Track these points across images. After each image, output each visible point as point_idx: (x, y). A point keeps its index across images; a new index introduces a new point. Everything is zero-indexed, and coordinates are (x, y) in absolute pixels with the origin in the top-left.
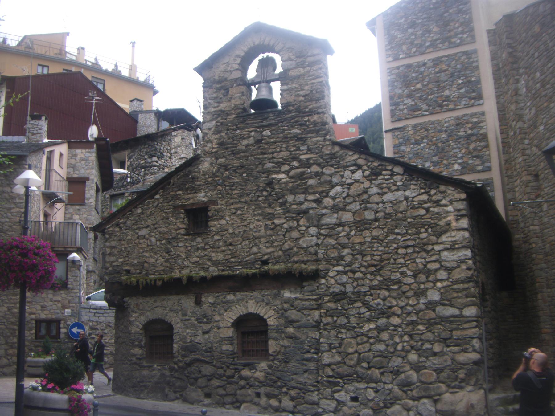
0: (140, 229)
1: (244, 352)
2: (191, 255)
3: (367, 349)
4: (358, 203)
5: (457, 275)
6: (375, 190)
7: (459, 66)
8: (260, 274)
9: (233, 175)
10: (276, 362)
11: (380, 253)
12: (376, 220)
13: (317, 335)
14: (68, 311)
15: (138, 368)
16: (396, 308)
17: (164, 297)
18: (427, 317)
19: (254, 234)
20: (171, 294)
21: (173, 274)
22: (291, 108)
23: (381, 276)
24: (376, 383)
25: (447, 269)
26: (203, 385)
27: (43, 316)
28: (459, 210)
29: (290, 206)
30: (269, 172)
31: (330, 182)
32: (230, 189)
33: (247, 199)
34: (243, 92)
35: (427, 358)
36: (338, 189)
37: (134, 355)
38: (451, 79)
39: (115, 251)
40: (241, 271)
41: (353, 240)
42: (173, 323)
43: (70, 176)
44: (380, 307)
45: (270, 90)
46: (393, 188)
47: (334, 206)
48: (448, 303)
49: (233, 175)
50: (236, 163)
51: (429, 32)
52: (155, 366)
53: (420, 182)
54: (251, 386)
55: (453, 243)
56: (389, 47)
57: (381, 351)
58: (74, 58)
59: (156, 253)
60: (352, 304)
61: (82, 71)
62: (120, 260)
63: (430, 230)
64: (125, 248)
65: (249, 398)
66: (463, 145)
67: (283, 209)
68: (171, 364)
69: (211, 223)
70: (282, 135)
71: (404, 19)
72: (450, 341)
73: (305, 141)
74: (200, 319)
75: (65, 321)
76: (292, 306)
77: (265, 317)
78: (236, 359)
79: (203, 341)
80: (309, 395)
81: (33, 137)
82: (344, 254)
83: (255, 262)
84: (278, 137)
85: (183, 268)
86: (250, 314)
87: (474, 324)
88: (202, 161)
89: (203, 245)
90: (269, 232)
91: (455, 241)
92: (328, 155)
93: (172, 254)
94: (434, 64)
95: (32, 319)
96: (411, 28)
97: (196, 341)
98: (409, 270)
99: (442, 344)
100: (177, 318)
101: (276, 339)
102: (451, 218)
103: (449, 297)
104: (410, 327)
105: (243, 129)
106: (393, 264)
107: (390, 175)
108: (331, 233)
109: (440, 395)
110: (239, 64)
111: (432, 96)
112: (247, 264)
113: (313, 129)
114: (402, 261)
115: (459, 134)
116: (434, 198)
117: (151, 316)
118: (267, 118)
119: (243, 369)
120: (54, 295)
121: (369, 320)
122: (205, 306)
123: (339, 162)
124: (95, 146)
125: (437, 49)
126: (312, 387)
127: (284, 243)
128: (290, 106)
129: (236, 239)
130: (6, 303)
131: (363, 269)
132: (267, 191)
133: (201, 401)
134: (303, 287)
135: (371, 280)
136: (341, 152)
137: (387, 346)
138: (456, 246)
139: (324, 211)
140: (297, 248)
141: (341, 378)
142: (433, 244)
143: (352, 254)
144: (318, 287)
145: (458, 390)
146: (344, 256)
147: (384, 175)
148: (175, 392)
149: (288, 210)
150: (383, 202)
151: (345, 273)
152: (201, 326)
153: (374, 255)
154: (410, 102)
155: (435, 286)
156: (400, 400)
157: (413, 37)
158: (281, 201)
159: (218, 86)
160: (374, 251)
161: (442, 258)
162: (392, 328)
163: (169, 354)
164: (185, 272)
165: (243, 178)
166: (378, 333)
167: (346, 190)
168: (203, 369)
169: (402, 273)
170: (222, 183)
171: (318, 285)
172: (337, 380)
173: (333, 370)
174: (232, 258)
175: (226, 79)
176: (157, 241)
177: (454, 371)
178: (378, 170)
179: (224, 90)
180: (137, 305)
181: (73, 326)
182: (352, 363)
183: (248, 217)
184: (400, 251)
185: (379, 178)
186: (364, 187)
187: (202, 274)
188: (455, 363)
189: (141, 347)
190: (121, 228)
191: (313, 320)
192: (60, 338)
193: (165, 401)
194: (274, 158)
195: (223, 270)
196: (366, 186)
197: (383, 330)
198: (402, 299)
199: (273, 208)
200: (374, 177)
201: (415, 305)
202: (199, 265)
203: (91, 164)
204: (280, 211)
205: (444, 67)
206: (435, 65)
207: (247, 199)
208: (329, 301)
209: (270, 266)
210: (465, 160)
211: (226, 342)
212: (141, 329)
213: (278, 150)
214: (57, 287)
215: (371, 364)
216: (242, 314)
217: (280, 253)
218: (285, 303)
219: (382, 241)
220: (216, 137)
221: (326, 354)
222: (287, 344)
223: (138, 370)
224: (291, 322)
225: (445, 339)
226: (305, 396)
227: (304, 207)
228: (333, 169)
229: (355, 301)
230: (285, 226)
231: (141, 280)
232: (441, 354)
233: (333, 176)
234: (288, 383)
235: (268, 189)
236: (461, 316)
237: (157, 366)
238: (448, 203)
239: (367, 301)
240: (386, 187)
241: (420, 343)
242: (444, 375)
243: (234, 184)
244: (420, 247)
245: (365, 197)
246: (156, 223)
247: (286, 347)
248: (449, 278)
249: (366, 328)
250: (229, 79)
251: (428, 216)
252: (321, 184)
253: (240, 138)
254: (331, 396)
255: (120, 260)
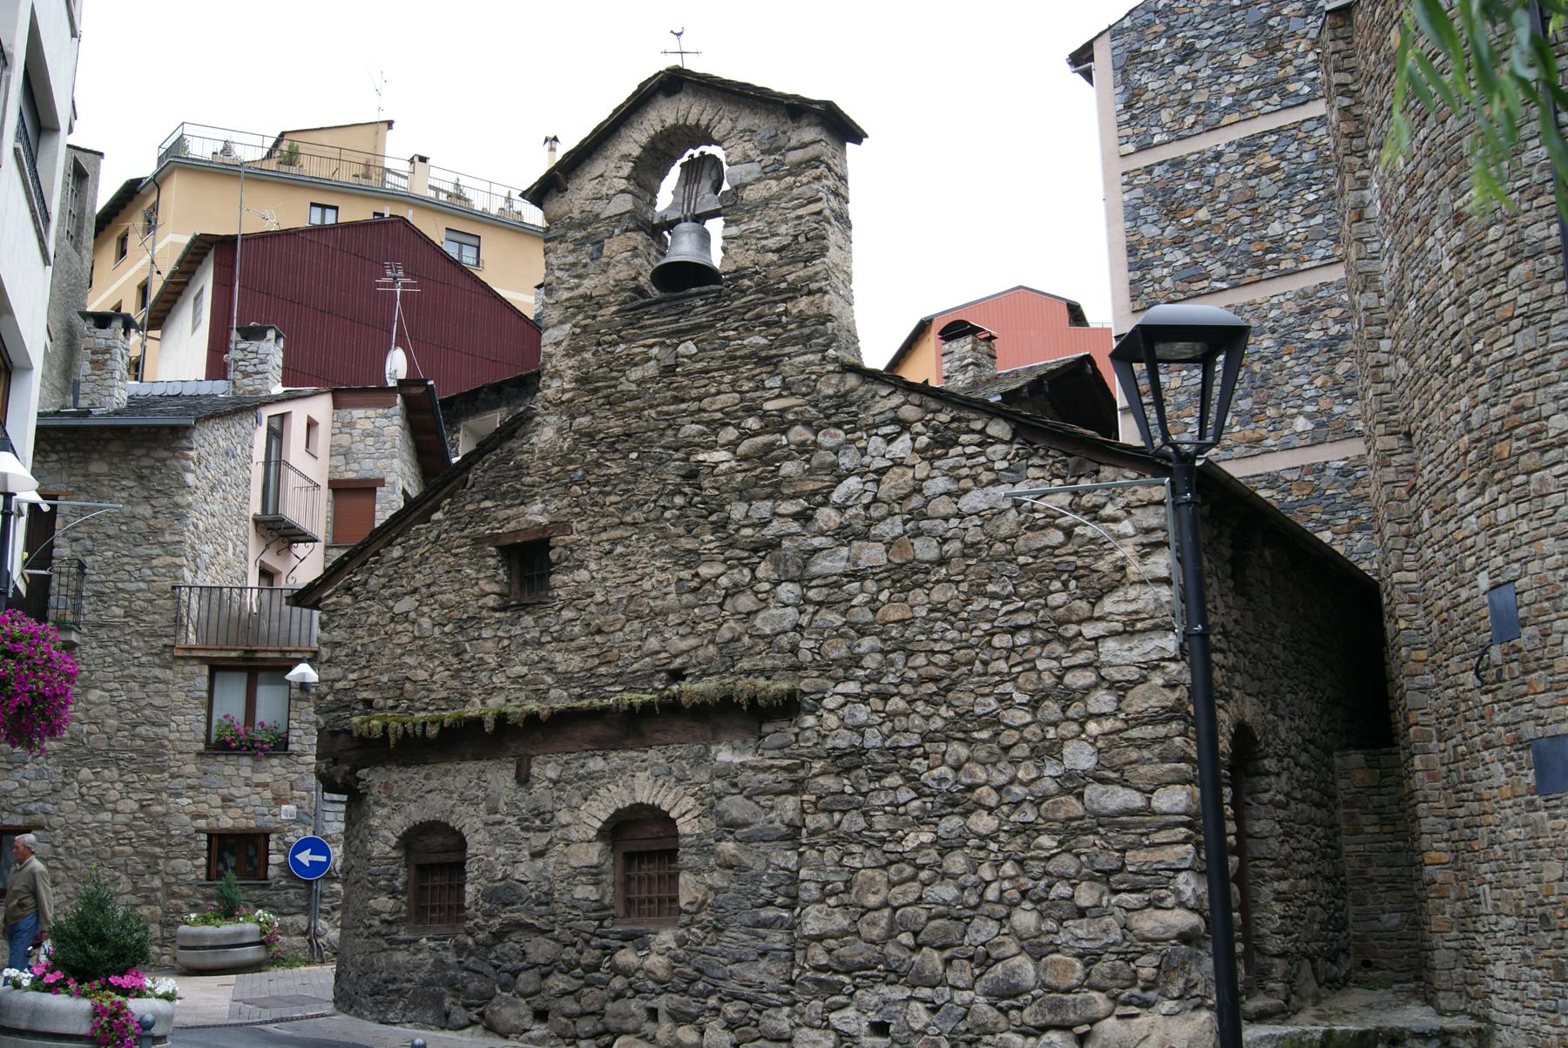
0: (396, 597)
1: (629, 903)
2: (509, 660)
3: (911, 898)
4: (898, 519)
5: (1138, 701)
6: (940, 484)
7: (1306, 157)
8: (661, 705)
9: (607, 456)
10: (694, 930)
11: (948, 647)
12: (943, 561)
13: (791, 860)
14: (288, 810)
15: (386, 946)
16: (985, 789)
17: (448, 767)
18: (1061, 815)
19: (652, 604)
20: (463, 759)
21: (468, 708)
22: (747, 282)
23: (950, 706)
24: (933, 987)
25: (1113, 686)
26: (530, 989)
27: (226, 822)
28: (1148, 531)
29: (737, 531)
30: (691, 446)
31: (835, 466)
32: (600, 492)
33: (639, 516)
34: (636, 248)
35: (1060, 921)
36: (853, 483)
37: (378, 913)
38: (1286, 192)
39: (341, 653)
40: (618, 696)
41: (885, 615)
42: (465, 831)
43: (337, 477)
44: (944, 787)
45: (705, 237)
46: (986, 476)
47: (842, 527)
48: (1113, 775)
49: (607, 456)
50: (615, 426)
51: (1230, 69)
52: (424, 940)
53: (1050, 461)
54: (638, 992)
55: (1133, 618)
56: (1126, 117)
57: (945, 903)
58: (403, 183)
59: (431, 657)
60: (879, 779)
61: (410, 215)
62: (352, 676)
63: (1073, 584)
64: (363, 645)
65: (630, 1024)
66: (1318, 364)
67: (722, 539)
68: (459, 937)
69: (556, 579)
70: (722, 353)
71: (1163, 41)
72: (1118, 877)
73: (776, 365)
74: (526, 820)
75: (282, 835)
76: (735, 785)
77: (672, 815)
78: (605, 923)
79: (532, 878)
80: (769, 1017)
81: (246, 381)
82: (861, 650)
83: (652, 675)
84: (713, 358)
85: (490, 692)
86: (638, 808)
87: (1182, 832)
88: (538, 424)
89: (537, 635)
90: (688, 598)
91: (1136, 612)
92: (830, 397)
93: (467, 657)
94: (1241, 155)
95: (199, 831)
96: (1181, 62)
97: (517, 877)
98: (1018, 688)
99: (1097, 885)
100: (475, 819)
101: (697, 871)
102: (1127, 550)
103: (1116, 761)
104: (1019, 840)
105: (635, 341)
106: (980, 675)
107: (979, 445)
108: (832, 599)
109: (1093, 1022)
110: (628, 178)
111: (1238, 239)
112: (635, 680)
113: (795, 333)
114: (1002, 666)
115: (1308, 336)
116: (1087, 500)
117: (416, 814)
118: (690, 311)
119: (623, 947)
120: (254, 771)
121: (919, 822)
122: (538, 788)
123: (856, 415)
124: (399, 399)
125: (1250, 115)
126: (776, 996)
127: (720, 625)
128: (743, 277)
129: (610, 617)
130: (136, 790)
131: (906, 689)
132: (685, 495)
133: (526, 1031)
134: (761, 738)
135: (927, 718)
136: (862, 389)
137: (963, 889)
138: (1139, 626)
139: (817, 542)
140: (751, 636)
141: (848, 973)
142: (1079, 622)
143: (882, 651)
144: (797, 735)
145: (1137, 1011)
146: (861, 657)
147: (964, 446)
148: (467, 1007)
149: (730, 540)
150: (961, 516)
151: (864, 699)
152: (527, 839)
153: (933, 652)
154: (1179, 257)
155: (1084, 731)
156: (993, 1034)
157: (1189, 86)
158: (714, 518)
159: (578, 235)
160: (935, 641)
161: (1103, 658)
162: (972, 842)
163: (456, 911)
164: (495, 702)
165: (628, 465)
166: (941, 855)
167: (870, 486)
168: (530, 949)
169: (1001, 699)
170: (583, 477)
171: (797, 730)
172: (836, 978)
173: (829, 951)
174: (601, 664)
175: (597, 215)
176: (434, 625)
177: (1128, 957)
178: (950, 433)
179: (593, 244)
180: (386, 786)
181: (301, 847)
182: (876, 933)
183: (638, 562)
184: (996, 641)
185: (952, 452)
186: (914, 478)
187: (533, 706)
188: (1130, 937)
189: (393, 893)
190: (355, 596)
191: (782, 822)
192: (266, 879)
193: (443, 1028)
194: (704, 411)
195: (581, 697)
196: (918, 476)
197: (952, 848)
198: (1000, 765)
199: (696, 537)
200: (939, 452)
201: (1033, 780)
202: (527, 684)
203: (388, 445)
204: (711, 546)
205: (1268, 160)
206: (1245, 157)
207: (639, 516)
208: (823, 773)
209: (685, 685)
210: (1324, 404)
211: (584, 879)
212: (394, 848)
213: (713, 390)
214: (263, 750)
215: (922, 936)
216: (620, 806)
217: (712, 649)
218: (719, 777)
219: (955, 614)
220: (572, 362)
221: (812, 910)
222: (720, 884)
223: (384, 950)
224: (731, 827)
225: (1108, 873)
226: (762, 1019)
227: (769, 532)
228: (841, 433)
229: (888, 772)
230: (724, 581)
231: (393, 724)
232: (1095, 912)
233: (841, 452)
234: (721, 983)
235: (687, 490)
236: (1148, 810)
237: (428, 939)
238: (1121, 513)
239: (915, 771)
240: (967, 476)
241: (1042, 883)
242: (1102, 967)
243: (608, 480)
244: (1046, 630)
245: (916, 501)
246: (434, 583)
247: (716, 891)
248: (1119, 709)
249: (910, 843)
250: (602, 216)
251: (1070, 548)
252: (810, 472)
253: (627, 363)
254: (823, 1020)
255: (352, 676)
